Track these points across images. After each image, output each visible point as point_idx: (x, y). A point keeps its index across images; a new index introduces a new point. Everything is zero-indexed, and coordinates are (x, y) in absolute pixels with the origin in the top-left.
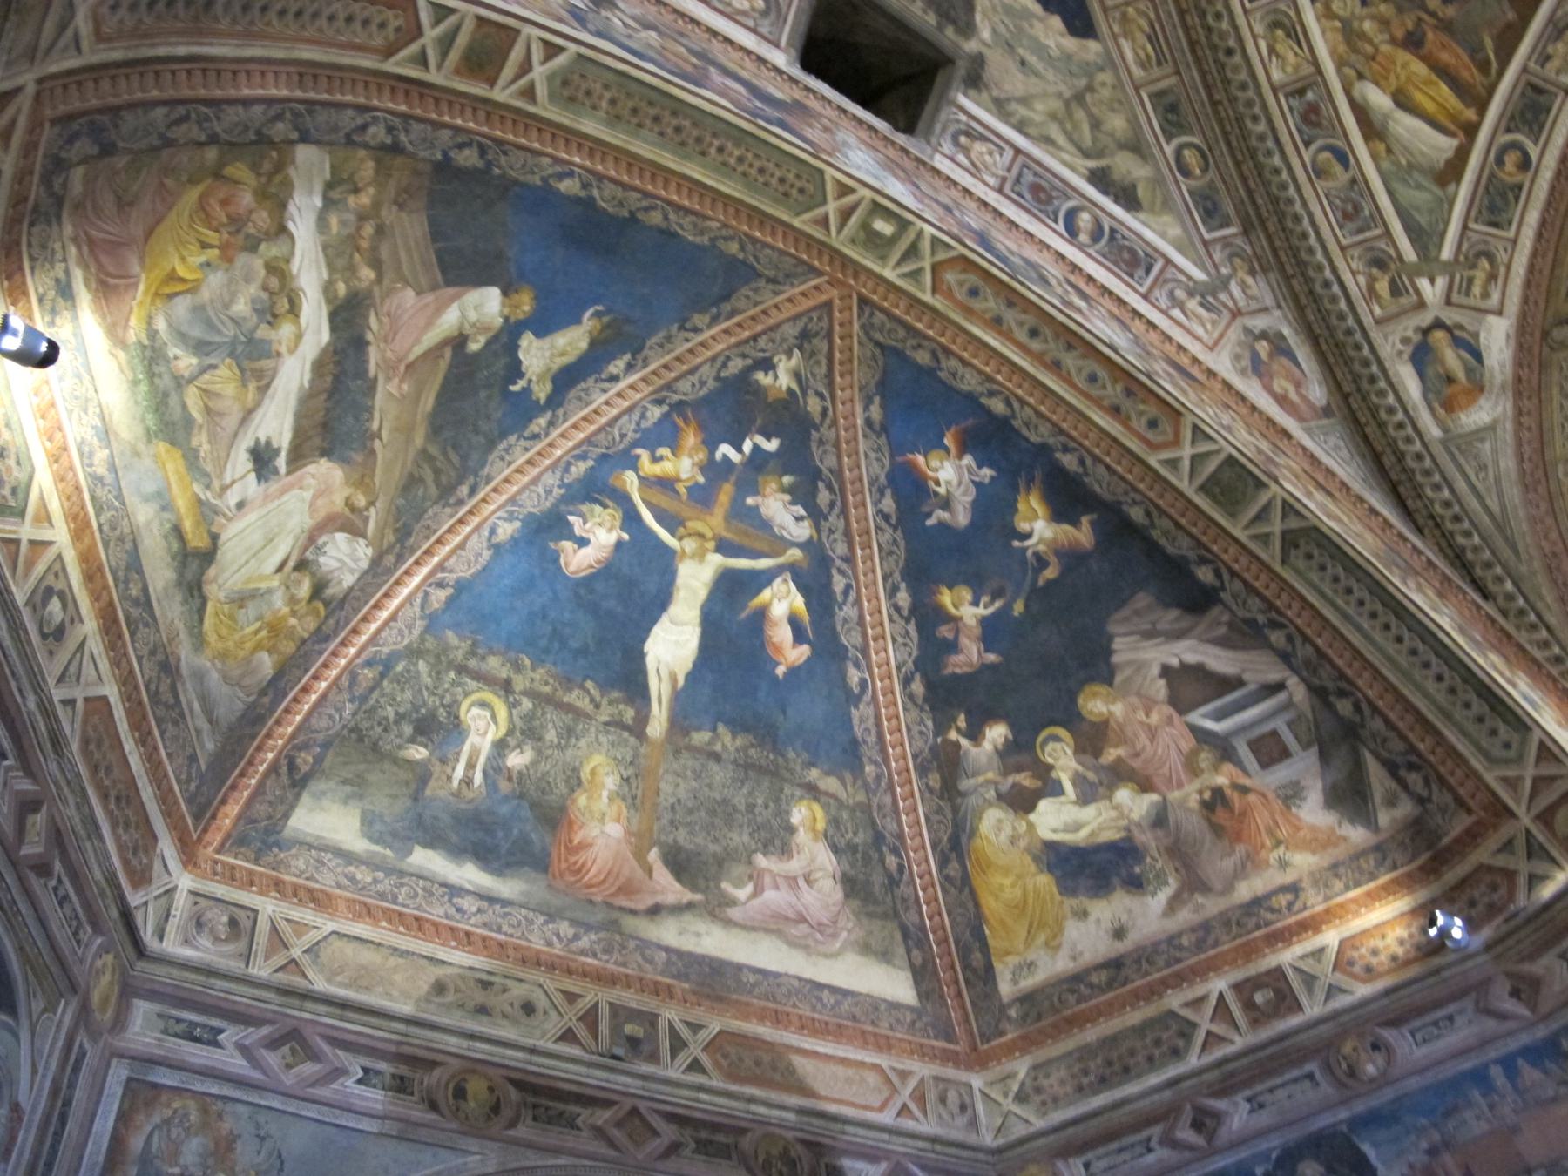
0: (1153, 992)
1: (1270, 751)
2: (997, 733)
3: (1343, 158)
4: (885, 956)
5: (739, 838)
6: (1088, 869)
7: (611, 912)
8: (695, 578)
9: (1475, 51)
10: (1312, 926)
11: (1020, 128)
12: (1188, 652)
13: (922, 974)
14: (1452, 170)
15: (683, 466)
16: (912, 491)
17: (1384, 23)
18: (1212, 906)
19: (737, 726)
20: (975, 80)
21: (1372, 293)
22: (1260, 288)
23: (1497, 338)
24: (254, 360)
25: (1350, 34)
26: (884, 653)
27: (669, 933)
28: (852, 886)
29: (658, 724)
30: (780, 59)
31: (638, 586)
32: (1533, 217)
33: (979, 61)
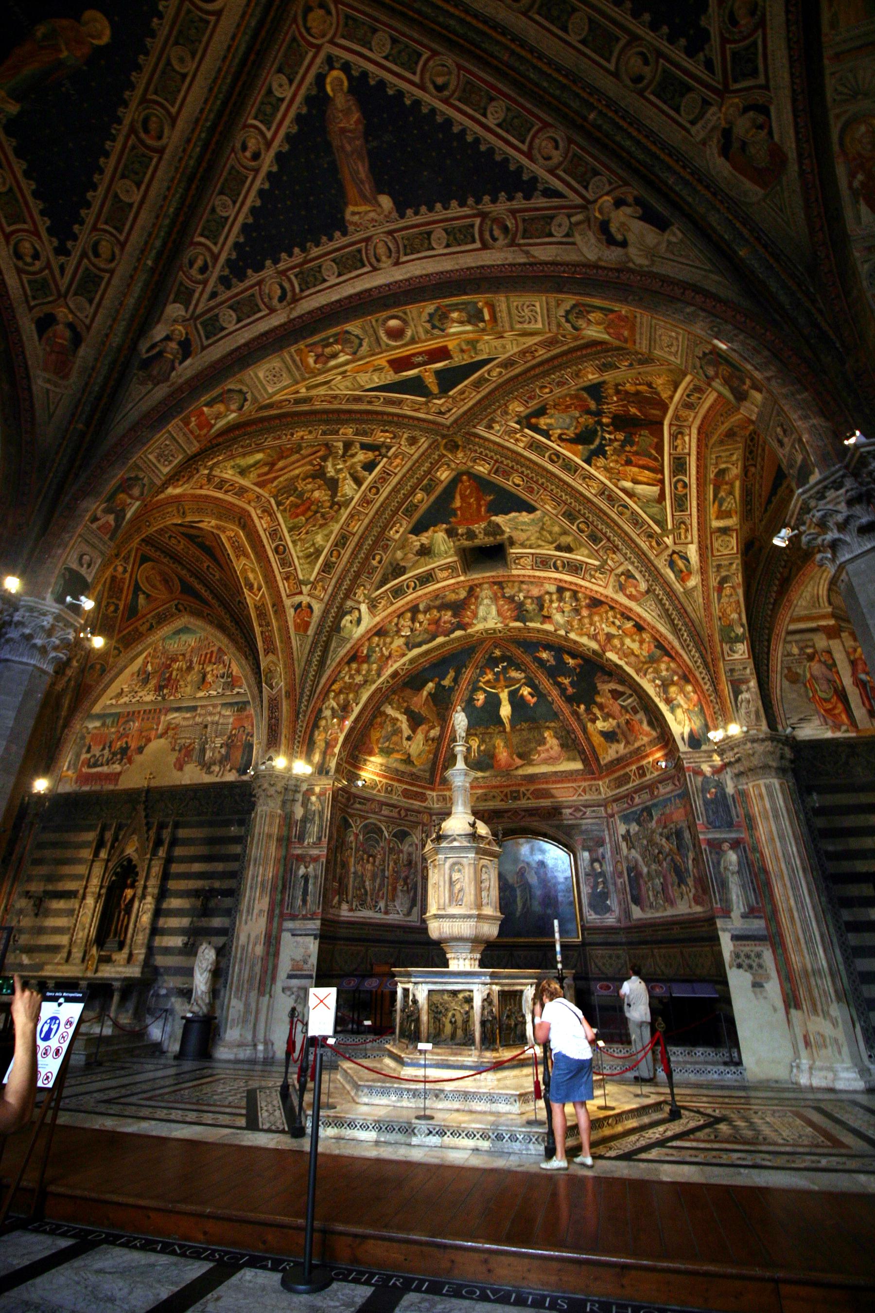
0: (624, 767)
1: (636, 712)
2: (582, 707)
3: (626, 507)
4: (574, 759)
5: (533, 745)
6: (610, 736)
7: (507, 772)
8: (504, 696)
9: (650, 456)
10: (647, 756)
11: (531, 547)
12: (613, 686)
13: (585, 761)
14: (662, 497)
15: (490, 676)
16: (541, 662)
17: (617, 461)
18: (632, 748)
19: (526, 721)
20: (512, 542)
21: (652, 547)
22: (618, 557)
23: (692, 552)
24: (398, 731)
25: (607, 469)
26: (555, 693)
27: (520, 772)
28: (562, 746)
29: (508, 729)
30: (462, 578)
31: (494, 702)
32: (694, 503)
33: (510, 538)
